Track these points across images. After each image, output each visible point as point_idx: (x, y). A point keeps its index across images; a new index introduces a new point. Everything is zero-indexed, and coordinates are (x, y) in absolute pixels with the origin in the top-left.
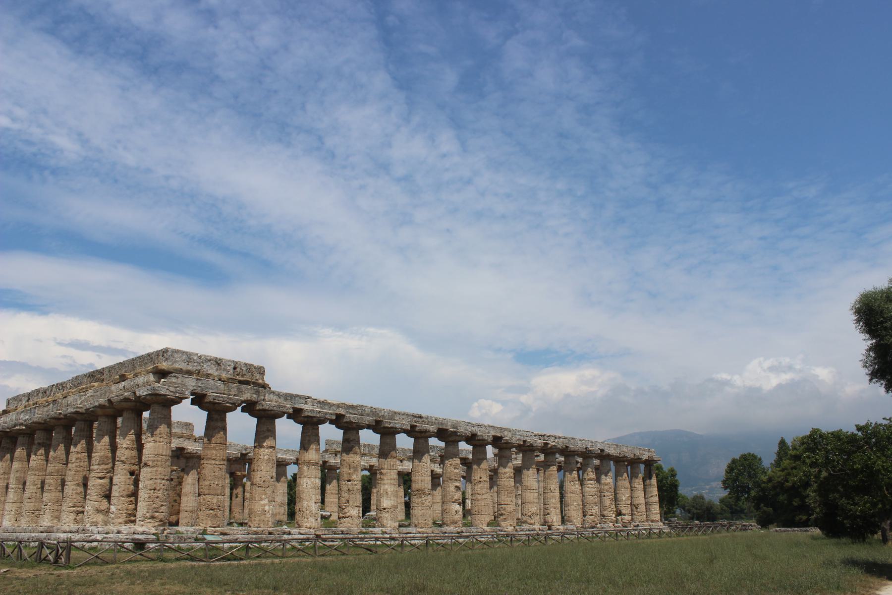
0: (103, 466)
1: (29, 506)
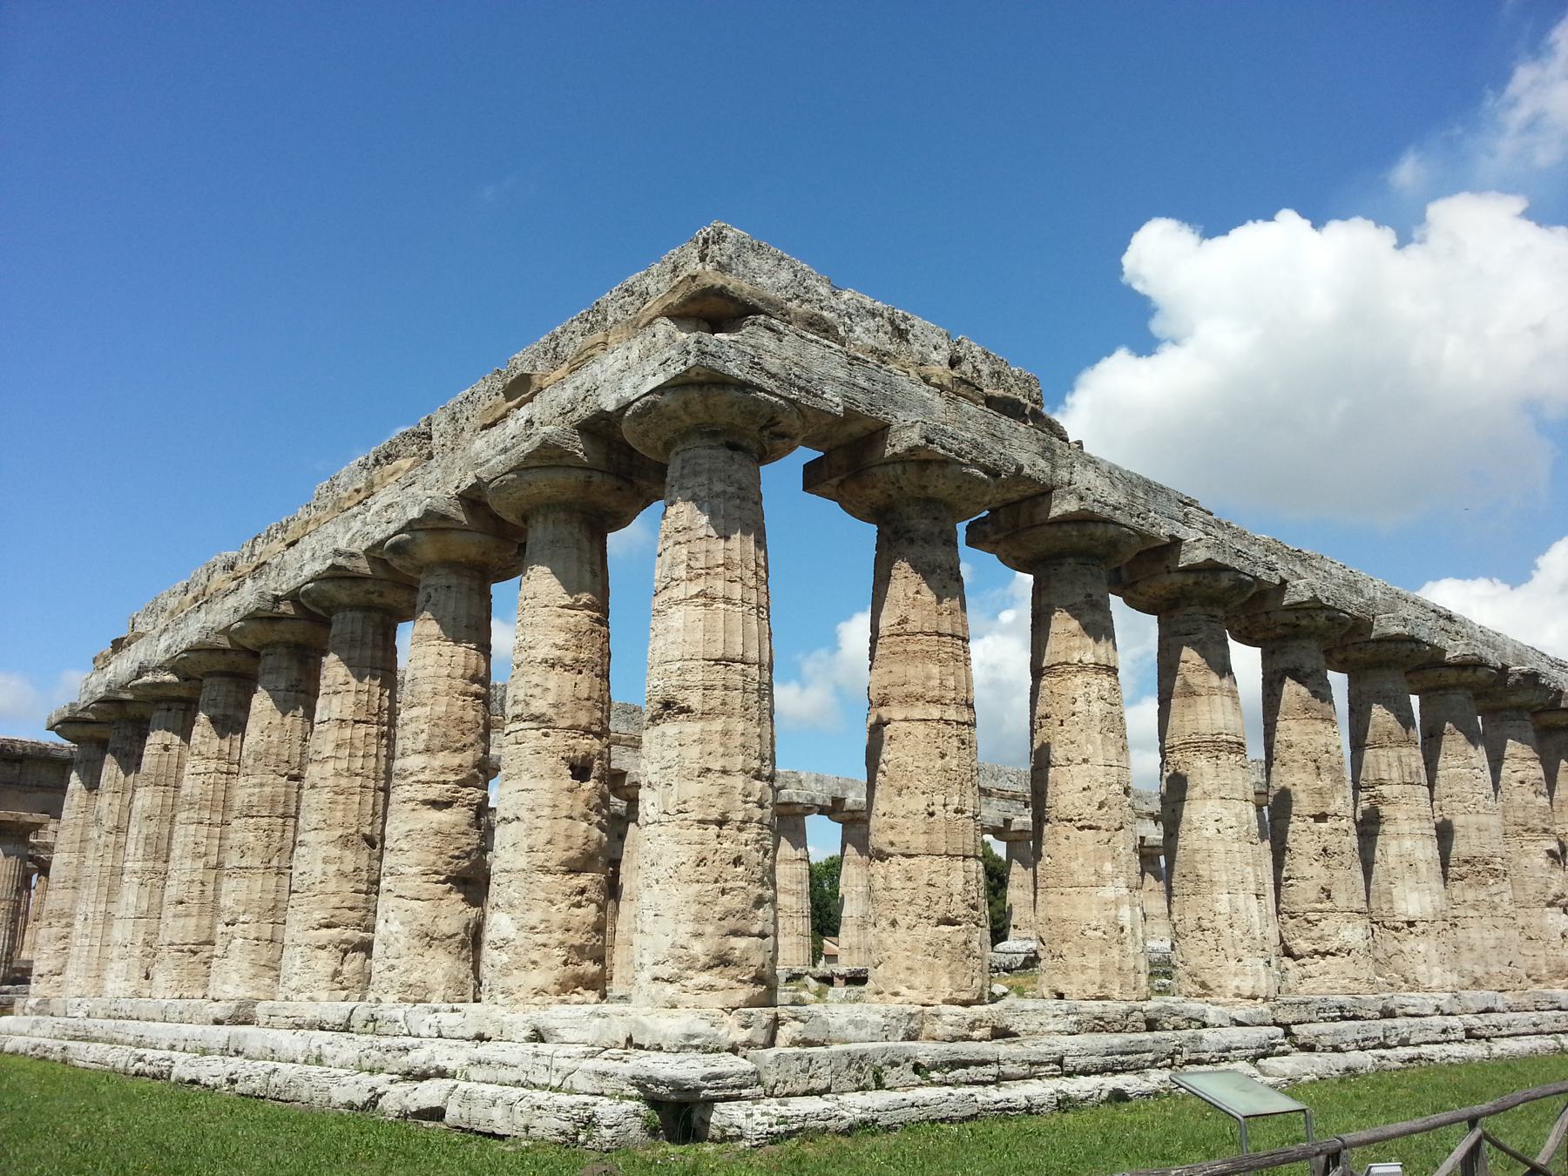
0: (444, 759)
1: (178, 928)
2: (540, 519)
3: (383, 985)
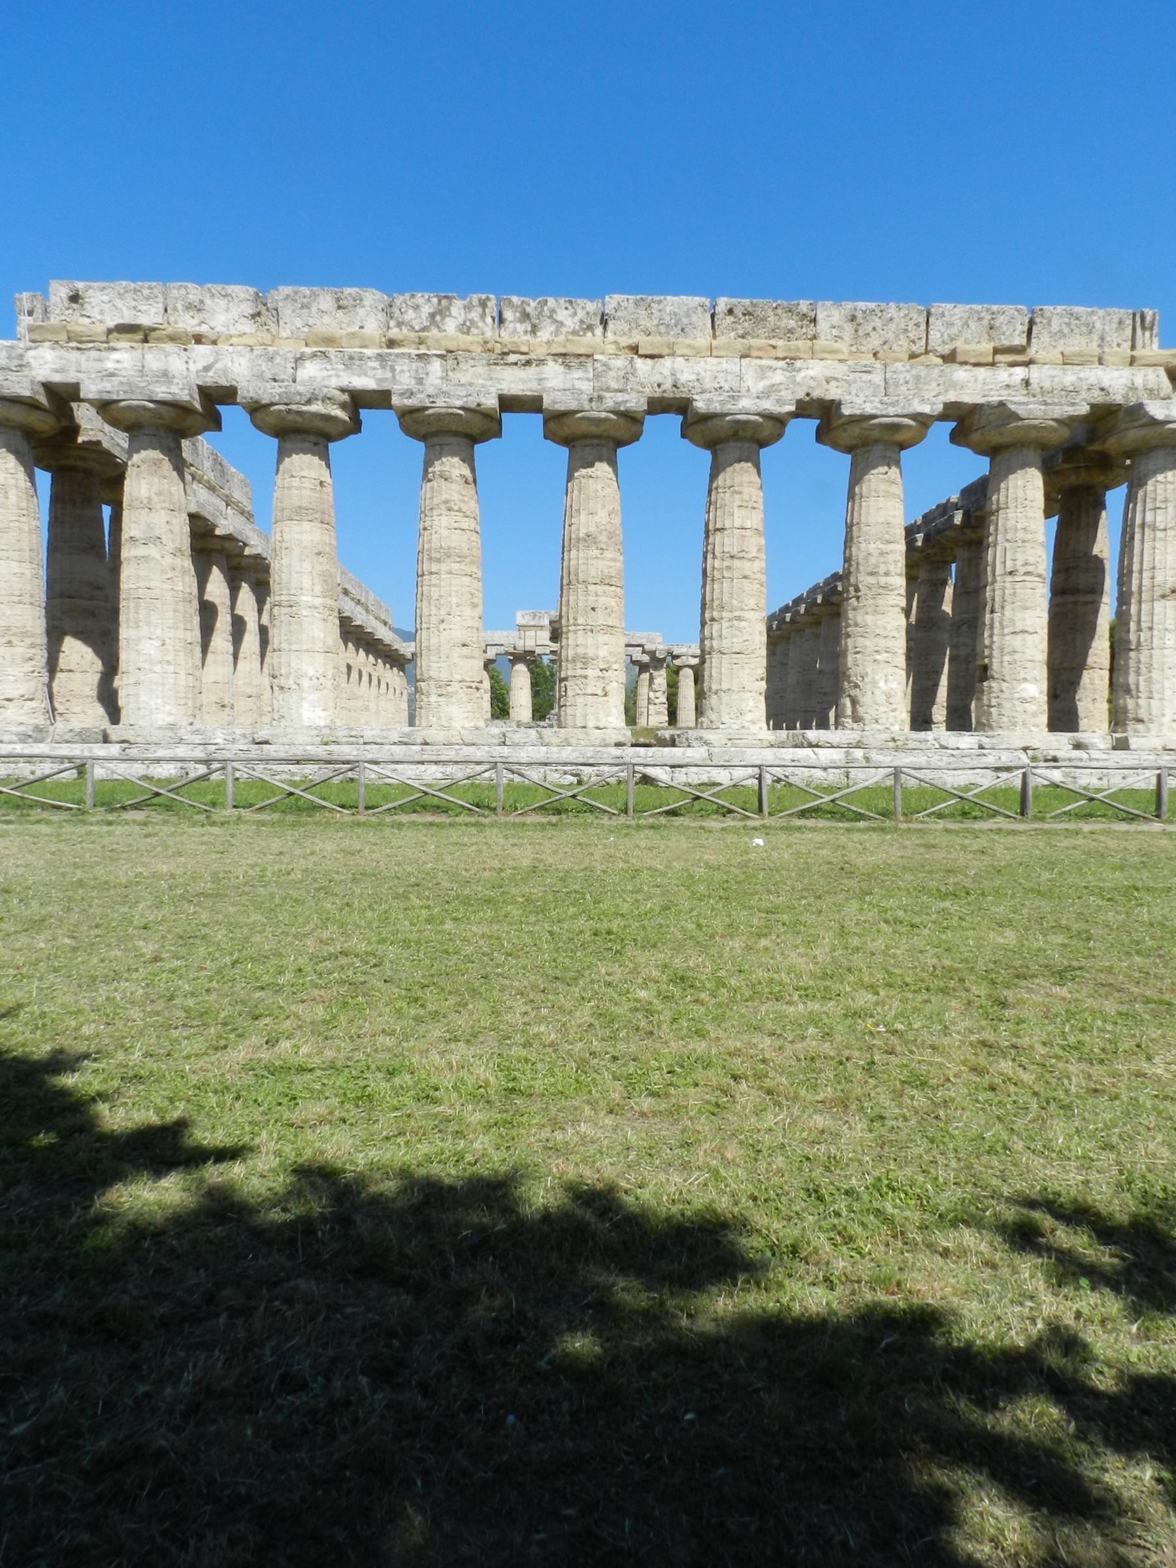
2: (1032, 450)
3: (891, 720)
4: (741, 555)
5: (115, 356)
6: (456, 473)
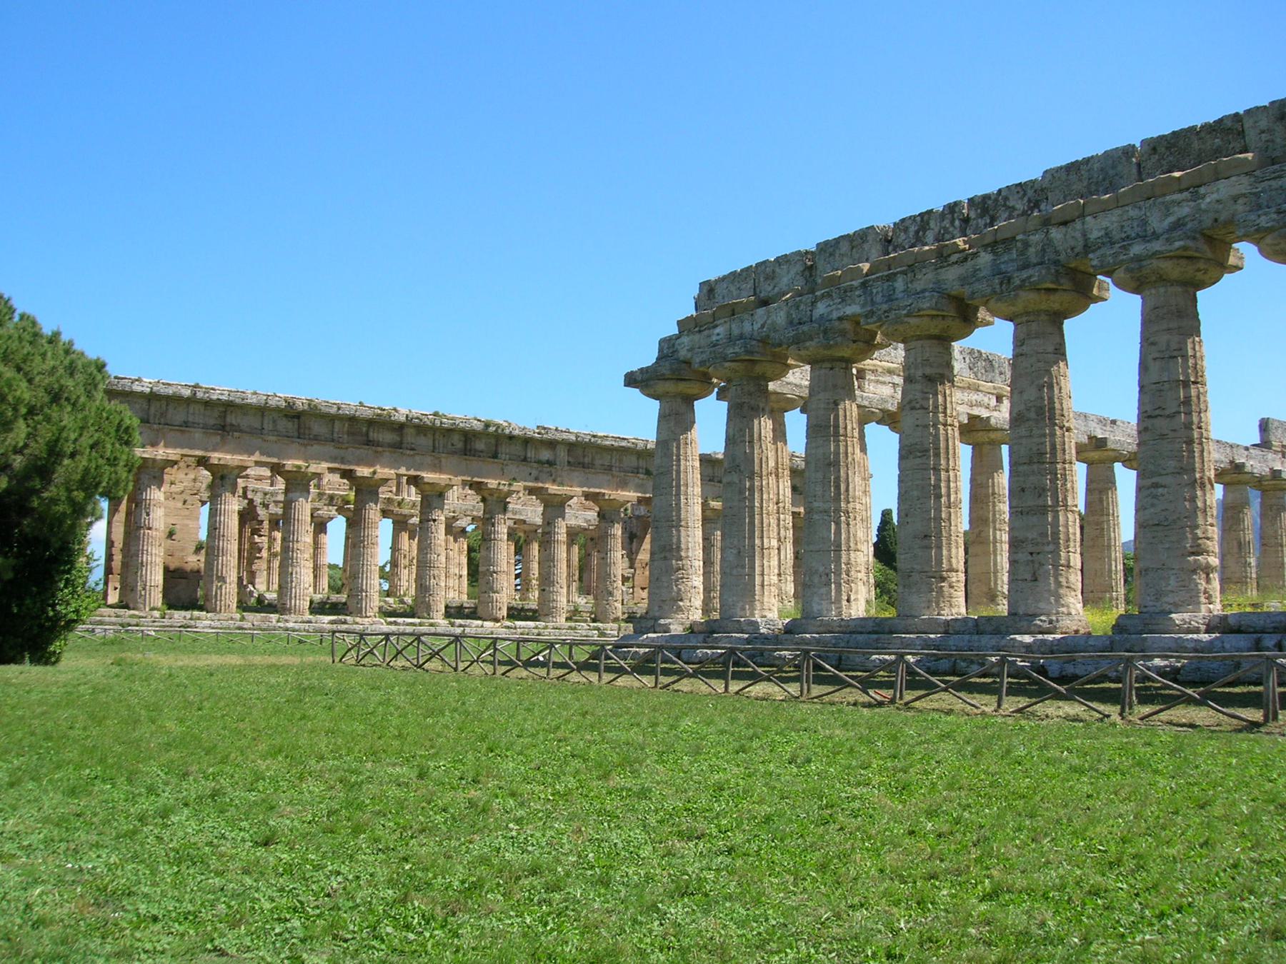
4: (1157, 412)
5: (717, 330)
6: (919, 373)
